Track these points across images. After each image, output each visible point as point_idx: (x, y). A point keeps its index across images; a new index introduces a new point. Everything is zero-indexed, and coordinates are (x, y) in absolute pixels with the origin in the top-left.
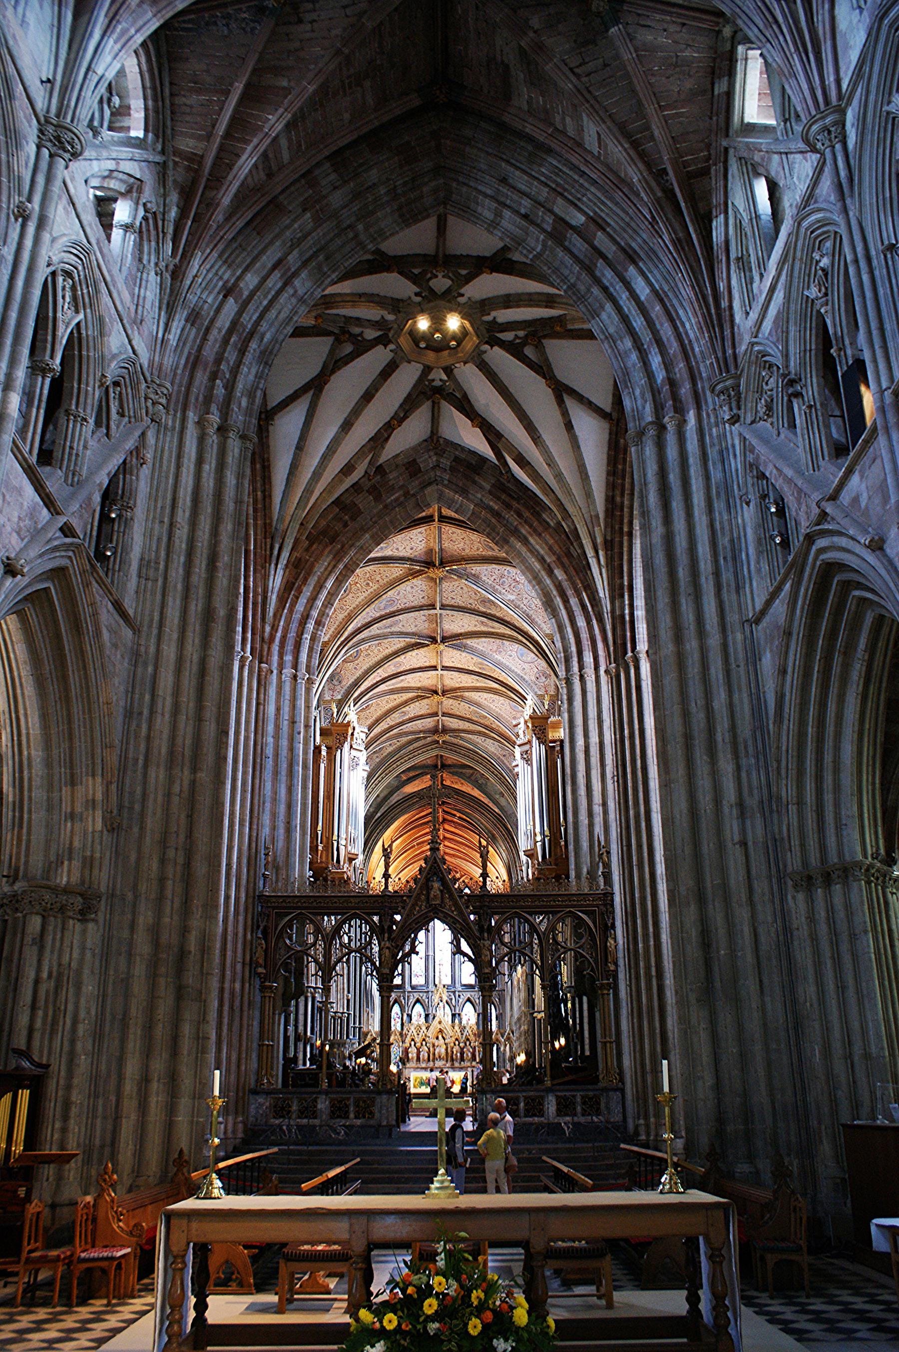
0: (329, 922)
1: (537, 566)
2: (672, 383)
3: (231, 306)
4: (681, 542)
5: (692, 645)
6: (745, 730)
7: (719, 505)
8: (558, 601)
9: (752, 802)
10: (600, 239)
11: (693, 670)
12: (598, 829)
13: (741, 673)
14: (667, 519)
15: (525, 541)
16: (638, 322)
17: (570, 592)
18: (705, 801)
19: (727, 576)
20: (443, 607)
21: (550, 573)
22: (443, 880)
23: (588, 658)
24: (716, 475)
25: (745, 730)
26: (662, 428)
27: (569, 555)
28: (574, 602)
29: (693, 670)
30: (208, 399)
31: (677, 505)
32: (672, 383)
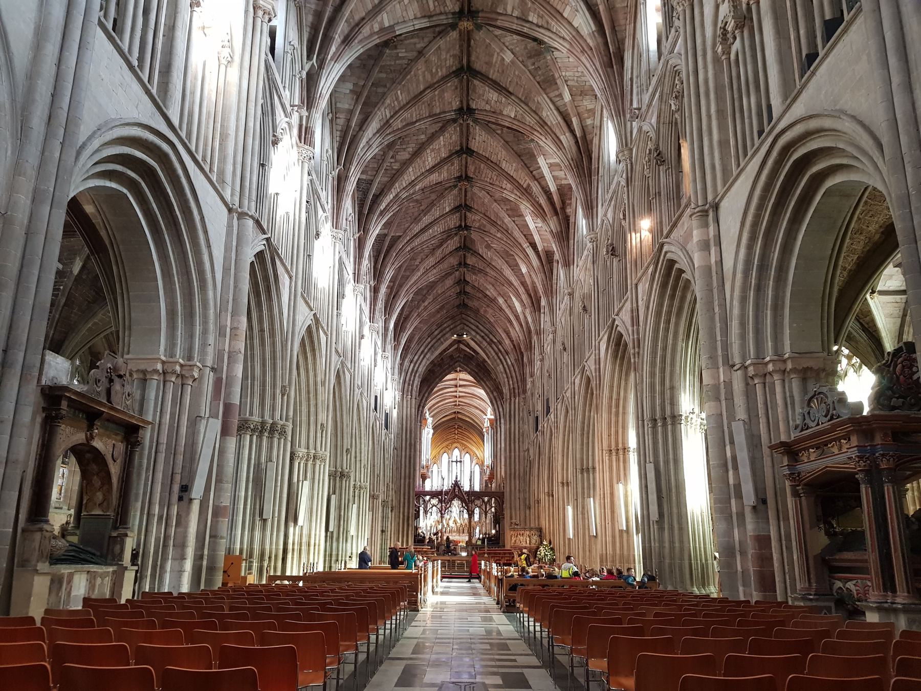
0: (428, 498)
1: (488, 390)
2: (514, 388)
3: (412, 365)
4: (513, 431)
5: (513, 454)
6: (522, 475)
7: (521, 422)
8: (494, 402)
9: (521, 490)
10: (500, 347)
11: (513, 460)
12: (503, 473)
13: (522, 461)
14: (510, 424)
15: (485, 383)
16: (508, 371)
17: (498, 400)
18: (513, 488)
19: (521, 439)
20: (460, 379)
21: (492, 393)
22: (459, 487)
23: (502, 421)
24: (521, 414)
25: (522, 475)
26: (511, 399)
27: (498, 388)
28: (499, 403)
29: (513, 460)
30: (408, 391)
31: (512, 420)
32: (514, 388)
